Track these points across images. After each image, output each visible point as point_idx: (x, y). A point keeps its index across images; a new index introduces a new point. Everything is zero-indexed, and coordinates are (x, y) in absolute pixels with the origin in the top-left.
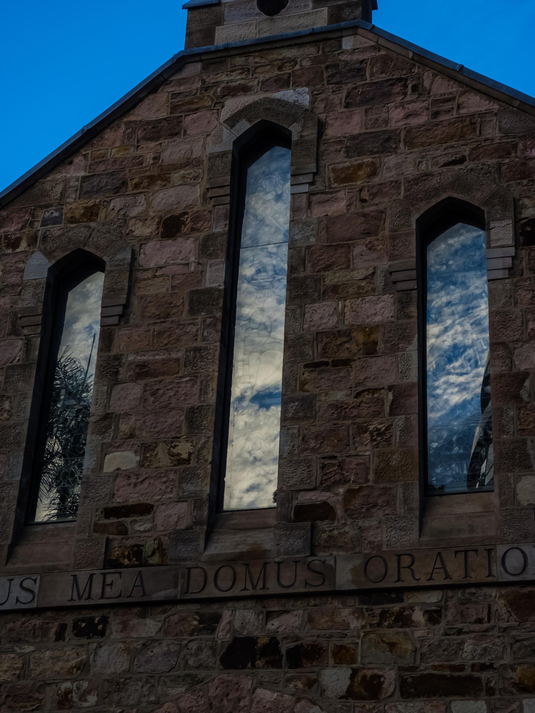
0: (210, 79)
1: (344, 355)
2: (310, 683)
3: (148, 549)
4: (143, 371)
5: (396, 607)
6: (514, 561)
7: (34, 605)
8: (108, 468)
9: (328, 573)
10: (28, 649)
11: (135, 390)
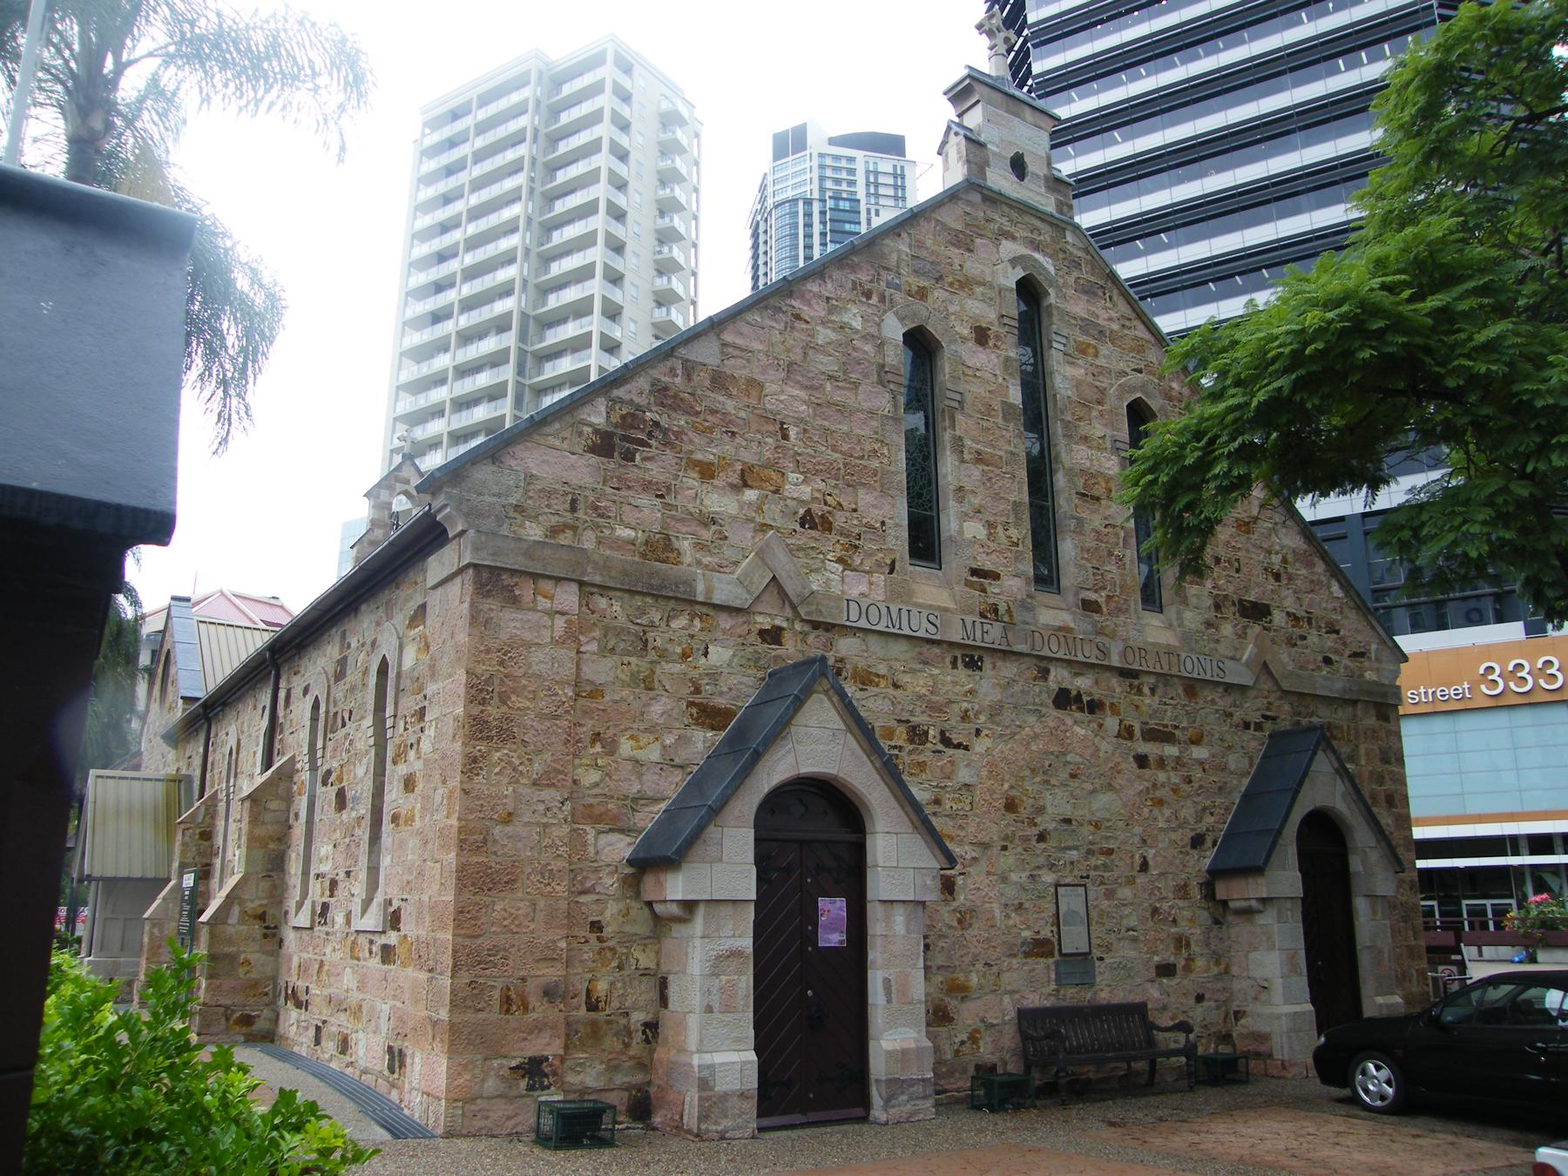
0: (990, 214)
1: (1096, 493)
2: (1101, 726)
3: (1002, 608)
4: (979, 459)
5: (1136, 682)
6: (1189, 667)
7: (938, 637)
8: (968, 535)
9: (1104, 653)
10: (936, 672)
11: (976, 472)
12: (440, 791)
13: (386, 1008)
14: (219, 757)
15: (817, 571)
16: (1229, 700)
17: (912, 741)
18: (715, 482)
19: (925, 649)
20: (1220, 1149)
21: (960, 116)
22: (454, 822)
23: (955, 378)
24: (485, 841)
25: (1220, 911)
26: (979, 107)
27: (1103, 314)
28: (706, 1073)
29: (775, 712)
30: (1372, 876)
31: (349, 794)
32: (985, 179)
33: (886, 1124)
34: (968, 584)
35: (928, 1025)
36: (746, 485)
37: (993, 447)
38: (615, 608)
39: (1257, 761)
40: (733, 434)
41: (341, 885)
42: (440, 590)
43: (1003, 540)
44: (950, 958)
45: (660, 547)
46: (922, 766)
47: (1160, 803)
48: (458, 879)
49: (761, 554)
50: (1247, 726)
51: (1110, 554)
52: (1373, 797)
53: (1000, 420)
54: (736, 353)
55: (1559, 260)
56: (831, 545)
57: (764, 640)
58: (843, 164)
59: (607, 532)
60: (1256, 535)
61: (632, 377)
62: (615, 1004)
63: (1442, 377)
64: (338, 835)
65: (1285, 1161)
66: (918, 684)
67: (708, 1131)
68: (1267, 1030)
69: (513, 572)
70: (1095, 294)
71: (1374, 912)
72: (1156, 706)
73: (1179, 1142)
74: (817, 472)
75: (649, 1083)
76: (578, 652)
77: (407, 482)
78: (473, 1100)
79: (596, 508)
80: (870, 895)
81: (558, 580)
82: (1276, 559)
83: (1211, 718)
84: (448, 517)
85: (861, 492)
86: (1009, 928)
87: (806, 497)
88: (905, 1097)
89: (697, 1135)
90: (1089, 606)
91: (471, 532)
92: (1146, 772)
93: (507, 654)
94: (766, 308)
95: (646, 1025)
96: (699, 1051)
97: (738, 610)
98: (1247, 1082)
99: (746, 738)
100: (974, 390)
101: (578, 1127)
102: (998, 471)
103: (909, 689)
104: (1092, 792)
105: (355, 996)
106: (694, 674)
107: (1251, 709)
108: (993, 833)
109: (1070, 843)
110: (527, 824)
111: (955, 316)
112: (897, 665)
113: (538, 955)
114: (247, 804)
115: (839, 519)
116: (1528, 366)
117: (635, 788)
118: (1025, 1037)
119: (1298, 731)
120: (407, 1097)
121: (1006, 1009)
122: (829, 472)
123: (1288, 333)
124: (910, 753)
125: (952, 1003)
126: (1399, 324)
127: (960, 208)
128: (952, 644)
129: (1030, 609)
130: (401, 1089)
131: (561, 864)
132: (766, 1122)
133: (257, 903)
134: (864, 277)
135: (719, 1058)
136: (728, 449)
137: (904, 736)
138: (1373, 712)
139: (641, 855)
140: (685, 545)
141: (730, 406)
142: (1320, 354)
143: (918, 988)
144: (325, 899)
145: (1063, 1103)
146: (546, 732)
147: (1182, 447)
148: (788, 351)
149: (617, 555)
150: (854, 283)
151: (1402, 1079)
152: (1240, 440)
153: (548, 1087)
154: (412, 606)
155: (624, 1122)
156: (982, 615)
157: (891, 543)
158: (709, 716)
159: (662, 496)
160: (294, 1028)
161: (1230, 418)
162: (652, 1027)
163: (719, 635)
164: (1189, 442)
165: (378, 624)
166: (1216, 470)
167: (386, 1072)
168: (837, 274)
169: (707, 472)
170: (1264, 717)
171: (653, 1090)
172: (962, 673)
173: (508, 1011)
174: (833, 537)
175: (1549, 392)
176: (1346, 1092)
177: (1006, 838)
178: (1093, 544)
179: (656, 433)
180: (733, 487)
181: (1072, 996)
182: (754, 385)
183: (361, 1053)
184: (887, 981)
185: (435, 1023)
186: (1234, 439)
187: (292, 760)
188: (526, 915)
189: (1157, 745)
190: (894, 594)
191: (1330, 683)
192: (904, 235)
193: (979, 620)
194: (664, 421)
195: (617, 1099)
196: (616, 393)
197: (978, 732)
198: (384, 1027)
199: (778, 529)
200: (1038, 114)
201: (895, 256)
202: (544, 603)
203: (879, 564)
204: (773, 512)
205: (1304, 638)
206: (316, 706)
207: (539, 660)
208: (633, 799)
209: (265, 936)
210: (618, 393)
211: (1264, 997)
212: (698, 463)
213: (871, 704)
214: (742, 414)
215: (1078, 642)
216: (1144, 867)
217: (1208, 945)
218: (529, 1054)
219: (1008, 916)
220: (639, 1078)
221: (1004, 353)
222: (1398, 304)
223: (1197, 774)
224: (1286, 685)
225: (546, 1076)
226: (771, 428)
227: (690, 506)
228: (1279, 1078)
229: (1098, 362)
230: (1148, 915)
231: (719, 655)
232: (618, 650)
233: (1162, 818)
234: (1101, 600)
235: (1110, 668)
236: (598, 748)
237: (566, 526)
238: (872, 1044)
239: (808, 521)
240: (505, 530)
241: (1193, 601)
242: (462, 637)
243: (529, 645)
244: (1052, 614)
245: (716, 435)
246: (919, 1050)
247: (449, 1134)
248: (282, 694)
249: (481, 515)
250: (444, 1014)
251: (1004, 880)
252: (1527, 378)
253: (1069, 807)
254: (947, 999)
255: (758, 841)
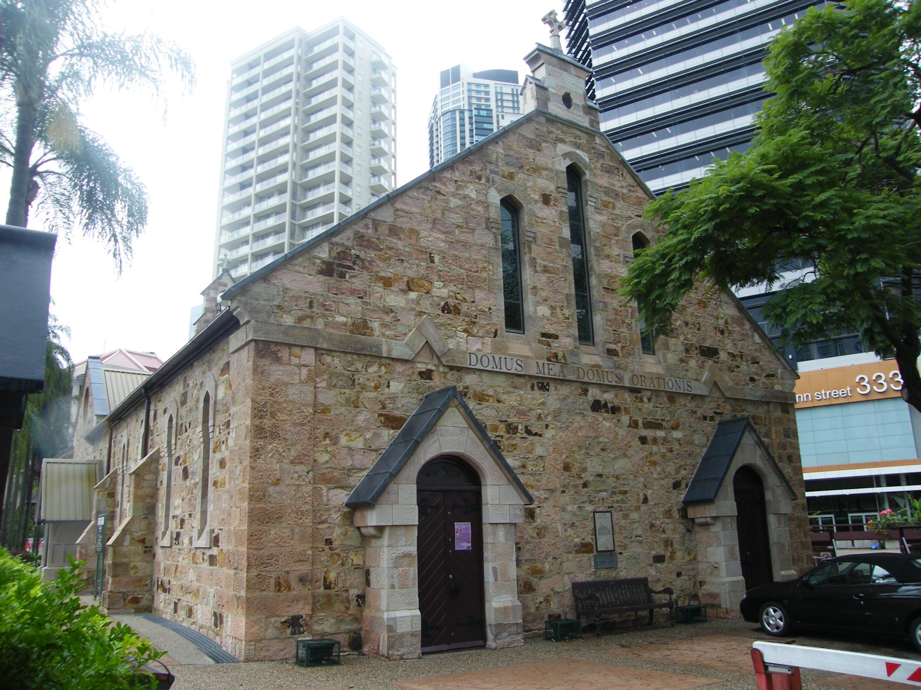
1: (614, 287)
2: (619, 421)
3: (560, 355)
4: (546, 270)
5: (639, 395)
6: (670, 384)
8: (540, 314)
9: (620, 379)
10: (522, 392)
11: (544, 278)
12: (239, 468)
13: (212, 591)
14: (118, 450)
15: (452, 337)
16: (694, 404)
17: (508, 432)
18: (392, 288)
19: (516, 380)
20: (680, 658)
21: (533, 72)
22: (246, 485)
23: (531, 225)
24: (264, 495)
25: (691, 525)
26: (543, 67)
27: (618, 184)
28: (391, 623)
29: (428, 418)
30: (778, 501)
31: (190, 470)
32: (547, 108)
33: (495, 649)
34: (540, 342)
35: (519, 593)
36: (410, 290)
37: (554, 263)
38: (336, 362)
39: (711, 438)
40: (402, 260)
41: (187, 522)
42: (237, 354)
43: (561, 316)
44: (533, 554)
45: (361, 327)
46: (514, 446)
47: (654, 463)
48: (249, 517)
49: (419, 329)
50: (705, 418)
51: (623, 322)
52: (780, 457)
53: (557, 248)
54: (403, 214)
55: (877, 148)
56: (460, 323)
57: (422, 378)
58: (482, 88)
59: (330, 319)
60: (704, 309)
61: (343, 231)
62: (340, 585)
63: (796, 222)
64: (184, 493)
65: (714, 664)
66: (511, 400)
67: (393, 655)
68: (717, 591)
69: (277, 343)
70: (613, 173)
71: (779, 523)
72: (651, 408)
73: (657, 655)
74: (451, 281)
75: (361, 629)
76: (315, 387)
77: (226, 285)
78: (260, 640)
79: (324, 306)
80: (484, 521)
81: (303, 347)
82: (721, 322)
83: (684, 414)
84: (239, 313)
85: (477, 291)
86: (567, 537)
87: (445, 295)
88: (506, 634)
89: (387, 658)
90: (611, 353)
91: (253, 322)
92: (646, 446)
93: (275, 389)
94: (420, 188)
95: (359, 596)
96: (387, 610)
97: (407, 361)
98: (705, 621)
99: (411, 433)
100: (542, 230)
101: (320, 655)
102: (556, 277)
103: (506, 403)
104: (615, 458)
105: (195, 585)
106: (382, 398)
107: (707, 408)
108: (557, 483)
109: (602, 488)
110: (288, 485)
111: (530, 189)
112: (499, 389)
113: (296, 559)
114: (133, 477)
115: (464, 307)
116: (845, 215)
117: (349, 463)
118: (576, 599)
119: (735, 420)
120: (224, 640)
121: (564, 584)
122: (458, 280)
123: (710, 198)
124: (508, 439)
125: (534, 580)
126: (772, 192)
127: (533, 125)
128: (531, 377)
129: (577, 355)
130: (221, 636)
131: (308, 507)
132: (427, 649)
133: (140, 533)
134: (477, 168)
135: (398, 614)
136: (400, 269)
137: (504, 429)
138: (779, 408)
139: (354, 501)
140: (376, 325)
141: (400, 245)
142: (725, 210)
143: (513, 571)
144: (178, 530)
145: (598, 635)
146: (298, 433)
147: (654, 263)
148: (433, 212)
149: (335, 331)
150: (471, 172)
151: (788, 617)
152: (685, 260)
153: (303, 633)
154: (222, 363)
155: (346, 652)
156: (549, 360)
157: (495, 320)
158: (391, 421)
159: (361, 298)
160: (162, 604)
161: (679, 247)
162: (362, 598)
163: (395, 375)
164: (658, 260)
165: (204, 373)
166: (672, 277)
167: (213, 627)
168: (461, 167)
169: (387, 283)
170: (715, 413)
171: (363, 633)
172: (537, 393)
173: (279, 590)
174: (461, 318)
175: (856, 230)
176: (758, 625)
177: (564, 486)
178: (613, 317)
179: (358, 262)
180: (402, 291)
181: (604, 575)
182: (414, 232)
183: (199, 617)
184: (494, 569)
185: (238, 598)
186: (681, 259)
187: (158, 451)
188: (288, 536)
189: (653, 431)
190: (497, 349)
191: (754, 392)
192: (500, 143)
193: (546, 362)
194: (362, 255)
195: (343, 639)
196: (334, 240)
197: (547, 426)
198: (211, 602)
199: (429, 314)
200: (578, 70)
201: (494, 156)
202: (295, 360)
203: (488, 332)
204: (426, 305)
205: (738, 367)
206: (171, 420)
207: (293, 393)
208: (349, 470)
209: (145, 552)
210: (336, 239)
211: (715, 572)
212: (382, 278)
213: (484, 412)
214: (407, 249)
215: (605, 374)
216: (645, 500)
217: (683, 544)
218: (292, 614)
219: (566, 530)
220: (355, 626)
221: (559, 209)
222: (771, 181)
223: (676, 447)
224: (728, 394)
225: (302, 626)
226: (424, 257)
227: (378, 303)
228: (725, 618)
229: (615, 212)
230: (648, 528)
231: (396, 387)
232: (338, 386)
233: (656, 472)
234: (618, 349)
235: (624, 388)
236: (328, 441)
237: (307, 317)
238: (487, 604)
239: (446, 309)
240: (272, 320)
241: (672, 348)
242: (249, 381)
243: (286, 384)
244: (590, 357)
245: (392, 261)
246: (514, 608)
247: (247, 660)
248: (152, 413)
249: (258, 312)
250: (243, 593)
251: (564, 510)
252: (843, 222)
253: (601, 467)
254: (531, 578)
255: (419, 491)
